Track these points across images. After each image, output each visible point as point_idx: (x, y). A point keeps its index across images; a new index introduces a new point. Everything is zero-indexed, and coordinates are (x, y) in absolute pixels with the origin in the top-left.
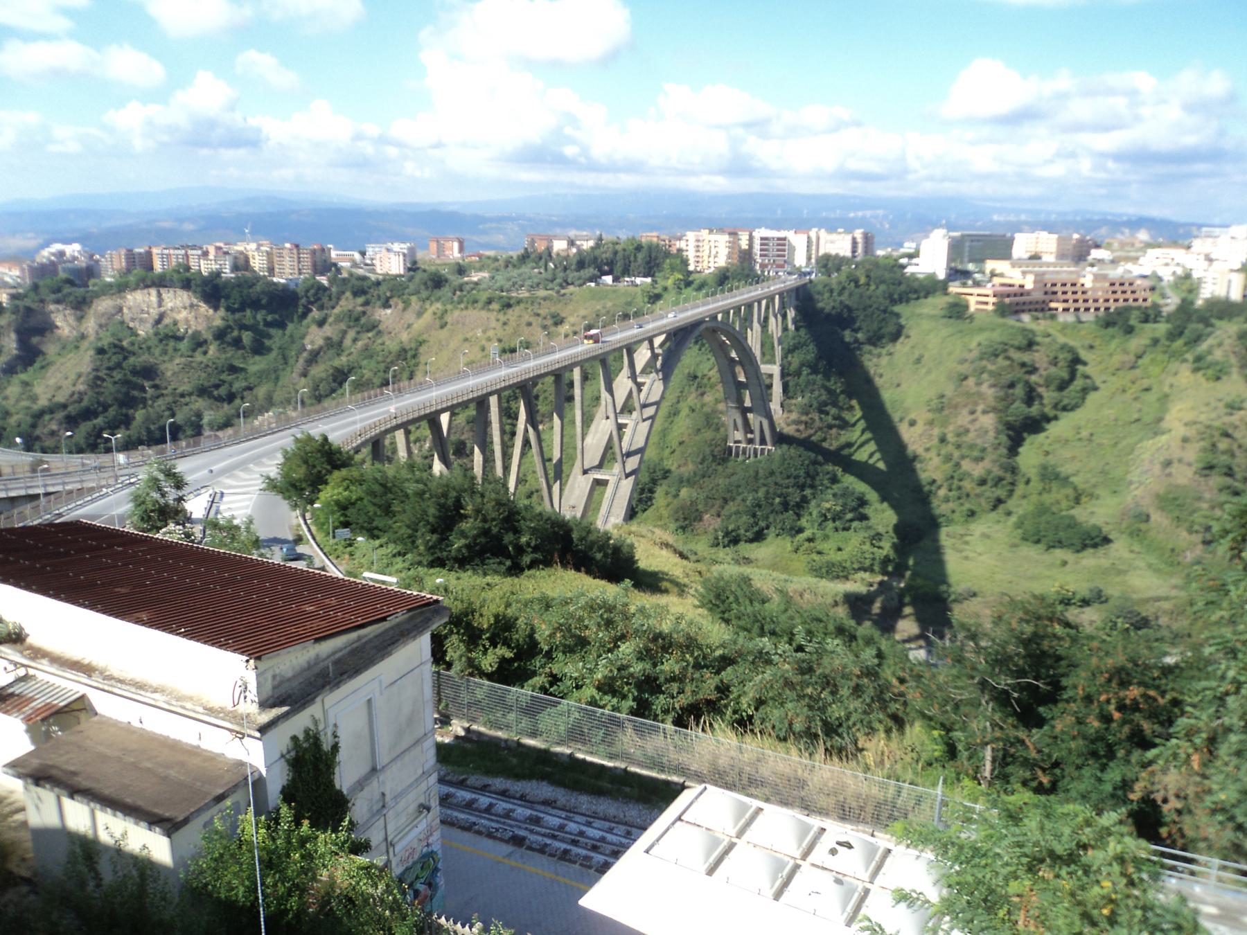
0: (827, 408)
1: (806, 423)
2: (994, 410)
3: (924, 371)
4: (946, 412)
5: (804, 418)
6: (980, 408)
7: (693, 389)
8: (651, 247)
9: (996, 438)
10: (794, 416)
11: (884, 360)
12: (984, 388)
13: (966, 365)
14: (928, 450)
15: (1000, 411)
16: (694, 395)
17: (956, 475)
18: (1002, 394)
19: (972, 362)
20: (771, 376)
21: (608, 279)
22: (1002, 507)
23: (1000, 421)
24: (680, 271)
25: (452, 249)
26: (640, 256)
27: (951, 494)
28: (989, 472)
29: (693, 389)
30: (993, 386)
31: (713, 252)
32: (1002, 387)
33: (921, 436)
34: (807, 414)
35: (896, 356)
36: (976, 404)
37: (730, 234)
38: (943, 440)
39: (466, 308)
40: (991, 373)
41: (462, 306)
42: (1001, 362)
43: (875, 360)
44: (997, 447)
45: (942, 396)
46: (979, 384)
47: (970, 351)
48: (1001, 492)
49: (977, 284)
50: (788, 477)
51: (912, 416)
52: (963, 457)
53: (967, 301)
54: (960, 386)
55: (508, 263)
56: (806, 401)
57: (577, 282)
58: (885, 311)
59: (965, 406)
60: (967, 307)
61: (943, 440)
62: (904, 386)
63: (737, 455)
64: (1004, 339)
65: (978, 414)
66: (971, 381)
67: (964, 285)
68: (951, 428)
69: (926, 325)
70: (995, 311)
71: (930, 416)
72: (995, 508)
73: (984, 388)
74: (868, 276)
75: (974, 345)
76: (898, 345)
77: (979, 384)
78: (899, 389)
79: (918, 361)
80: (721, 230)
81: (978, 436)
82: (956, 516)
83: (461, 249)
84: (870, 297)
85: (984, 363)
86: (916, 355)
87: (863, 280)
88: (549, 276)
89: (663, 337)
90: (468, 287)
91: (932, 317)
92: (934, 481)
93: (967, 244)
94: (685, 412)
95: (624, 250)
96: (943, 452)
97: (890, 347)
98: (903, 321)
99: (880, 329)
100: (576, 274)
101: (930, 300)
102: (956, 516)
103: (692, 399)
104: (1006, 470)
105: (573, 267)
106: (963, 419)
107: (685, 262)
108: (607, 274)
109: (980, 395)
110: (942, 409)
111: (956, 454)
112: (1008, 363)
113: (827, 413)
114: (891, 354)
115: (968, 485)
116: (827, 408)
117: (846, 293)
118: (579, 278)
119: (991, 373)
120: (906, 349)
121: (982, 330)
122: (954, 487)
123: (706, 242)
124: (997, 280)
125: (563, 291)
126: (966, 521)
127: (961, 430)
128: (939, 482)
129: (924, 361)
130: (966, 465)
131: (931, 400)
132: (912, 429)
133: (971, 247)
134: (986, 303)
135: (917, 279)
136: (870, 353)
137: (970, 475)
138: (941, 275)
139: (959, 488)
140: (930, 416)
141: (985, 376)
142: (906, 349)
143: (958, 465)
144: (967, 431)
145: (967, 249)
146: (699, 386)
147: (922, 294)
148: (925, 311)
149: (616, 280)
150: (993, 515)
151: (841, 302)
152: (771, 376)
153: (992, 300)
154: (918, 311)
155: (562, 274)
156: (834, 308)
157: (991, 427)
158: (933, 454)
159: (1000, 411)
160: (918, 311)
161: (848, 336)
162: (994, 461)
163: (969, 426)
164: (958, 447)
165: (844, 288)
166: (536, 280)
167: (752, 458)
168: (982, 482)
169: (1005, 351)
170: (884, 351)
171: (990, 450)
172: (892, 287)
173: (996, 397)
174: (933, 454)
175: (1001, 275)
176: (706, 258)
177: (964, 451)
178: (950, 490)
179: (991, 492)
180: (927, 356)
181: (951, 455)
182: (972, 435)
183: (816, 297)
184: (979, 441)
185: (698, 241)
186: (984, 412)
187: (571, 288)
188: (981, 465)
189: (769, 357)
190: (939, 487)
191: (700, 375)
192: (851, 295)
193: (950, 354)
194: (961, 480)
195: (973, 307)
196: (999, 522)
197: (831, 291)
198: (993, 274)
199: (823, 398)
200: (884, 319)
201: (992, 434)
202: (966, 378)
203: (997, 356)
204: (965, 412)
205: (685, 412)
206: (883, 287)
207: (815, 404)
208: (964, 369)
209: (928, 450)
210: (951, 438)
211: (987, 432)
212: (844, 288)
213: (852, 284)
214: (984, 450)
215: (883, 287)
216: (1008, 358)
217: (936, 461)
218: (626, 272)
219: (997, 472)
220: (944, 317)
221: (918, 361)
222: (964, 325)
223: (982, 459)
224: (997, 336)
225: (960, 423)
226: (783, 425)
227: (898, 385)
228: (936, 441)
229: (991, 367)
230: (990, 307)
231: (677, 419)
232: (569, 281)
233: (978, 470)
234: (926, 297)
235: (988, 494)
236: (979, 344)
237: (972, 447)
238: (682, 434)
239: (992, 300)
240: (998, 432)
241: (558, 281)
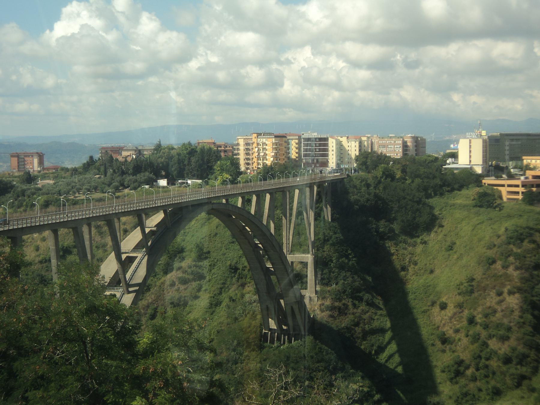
0: (361, 295)
1: (340, 308)
2: (520, 290)
3: (455, 256)
4: (476, 294)
5: (337, 304)
6: (506, 290)
7: (234, 280)
8: (202, 150)
9: (521, 317)
10: (328, 302)
11: (419, 249)
12: (511, 270)
13: (496, 249)
14: (457, 331)
15: (526, 291)
16: (235, 286)
17: (483, 355)
18: (527, 275)
19: (499, 247)
20: (305, 264)
21: (163, 182)
22: (526, 382)
23: (525, 300)
24: (228, 171)
25: (32, 163)
26: (193, 160)
27: (477, 374)
28: (514, 350)
29: (234, 280)
30: (517, 269)
31: (262, 154)
32: (527, 269)
33: (451, 318)
34: (340, 300)
35: (431, 244)
36: (503, 285)
37: (276, 137)
38: (471, 321)
39: (25, 211)
40: (518, 257)
41: (22, 209)
42: (527, 245)
43: (410, 249)
44: (521, 325)
45: (473, 280)
46: (505, 267)
47: (499, 237)
48: (524, 370)
49: (511, 177)
50: (319, 362)
51: (444, 300)
52: (490, 337)
53: (500, 192)
54: (489, 268)
55: (75, 171)
56: (339, 287)
57: (132, 186)
58: (419, 202)
59: (494, 288)
60: (501, 197)
61: (471, 321)
62: (437, 272)
63: (272, 342)
64: (531, 224)
65: (505, 295)
66: (498, 265)
67: (498, 177)
68: (480, 309)
69: (458, 214)
70: (523, 200)
71: (460, 299)
72: (518, 385)
73: (511, 270)
74: (404, 171)
75: (503, 229)
76: (433, 235)
77: (505, 267)
78: (432, 276)
79: (451, 248)
80: (267, 134)
81: (504, 316)
82: (483, 395)
83: (41, 163)
84: (404, 190)
85: (511, 246)
86: (448, 244)
87: (398, 175)
88: (107, 179)
89: (159, 217)
90: (28, 192)
91: (465, 206)
92: (462, 361)
93: (507, 143)
94: (226, 302)
95: (179, 154)
96: (471, 333)
97: (425, 237)
98: (436, 212)
99: (414, 218)
100: (131, 177)
101: (464, 192)
102: (483, 395)
103: (233, 291)
104: (531, 347)
105: (131, 171)
106: (491, 300)
107: (235, 164)
108: (162, 177)
109: (508, 277)
110: (472, 292)
111: (484, 334)
112: (533, 246)
113: (361, 299)
114: (425, 243)
115: (494, 363)
116: (361, 295)
117: (381, 187)
118: (136, 181)
119: (518, 257)
120: (440, 237)
121: (509, 216)
122: (481, 365)
123: (255, 145)
124: (529, 173)
125: (117, 194)
126: (492, 399)
127: (490, 311)
128: (467, 362)
129: (455, 248)
130: (493, 344)
131: (462, 284)
132: (443, 312)
133: (510, 145)
134: (517, 193)
135: (454, 174)
136: (405, 242)
137: (496, 353)
138: (479, 170)
139: (487, 367)
140: (460, 299)
141: (511, 259)
142: (440, 237)
143: (485, 345)
144: (495, 311)
145: (507, 148)
146: (240, 277)
147: (456, 186)
148: (459, 202)
149: (171, 182)
150: (518, 392)
151: (376, 195)
152: (305, 264)
153: (521, 189)
154: (451, 202)
155: (119, 179)
156: (368, 200)
157: (516, 307)
158: (462, 335)
159: (526, 291)
160: (451, 202)
161: (382, 225)
162: (518, 339)
163: (496, 307)
164: (486, 327)
165: (380, 182)
166: (93, 184)
167: (286, 344)
168: (507, 361)
169: (531, 235)
170: (419, 240)
171: (515, 328)
172: (426, 180)
173: (522, 279)
174: (462, 335)
175: (534, 169)
176: (255, 160)
177: (492, 331)
178: (477, 370)
179: (514, 369)
180: (458, 243)
181: (479, 334)
182: (499, 315)
183: (351, 190)
184: (506, 321)
185: (247, 144)
186: (510, 293)
187: (126, 191)
188: (507, 343)
189: (298, 246)
190: (468, 368)
191: (240, 267)
192: (385, 188)
193: (480, 240)
194: (488, 359)
195: (505, 197)
196: (523, 398)
197: (368, 186)
198: (528, 168)
199: (357, 284)
200: (417, 210)
201: (517, 313)
202: (494, 262)
203: (522, 241)
204: (493, 293)
205: (226, 302)
206: (418, 181)
207: (349, 291)
208: (490, 253)
209: (457, 331)
210: (479, 318)
211: (513, 311)
212: (380, 182)
213: (389, 180)
214: (509, 329)
215: (418, 181)
216: (534, 242)
217: (465, 341)
218: (181, 175)
219: (521, 349)
220: (476, 206)
221: (451, 248)
222: (494, 214)
223: (508, 338)
224: (522, 222)
225: (488, 304)
226: (318, 312)
227: (432, 272)
228: (465, 323)
229: (515, 250)
230: (520, 197)
231: (218, 309)
232: (126, 183)
233: (504, 349)
234: (460, 190)
235: (513, 371)
236: (506, 229)
237: (498, 326)
238: (221, 323)
239: (521, 189)
240: (523, 311)
241: (116, 184)
